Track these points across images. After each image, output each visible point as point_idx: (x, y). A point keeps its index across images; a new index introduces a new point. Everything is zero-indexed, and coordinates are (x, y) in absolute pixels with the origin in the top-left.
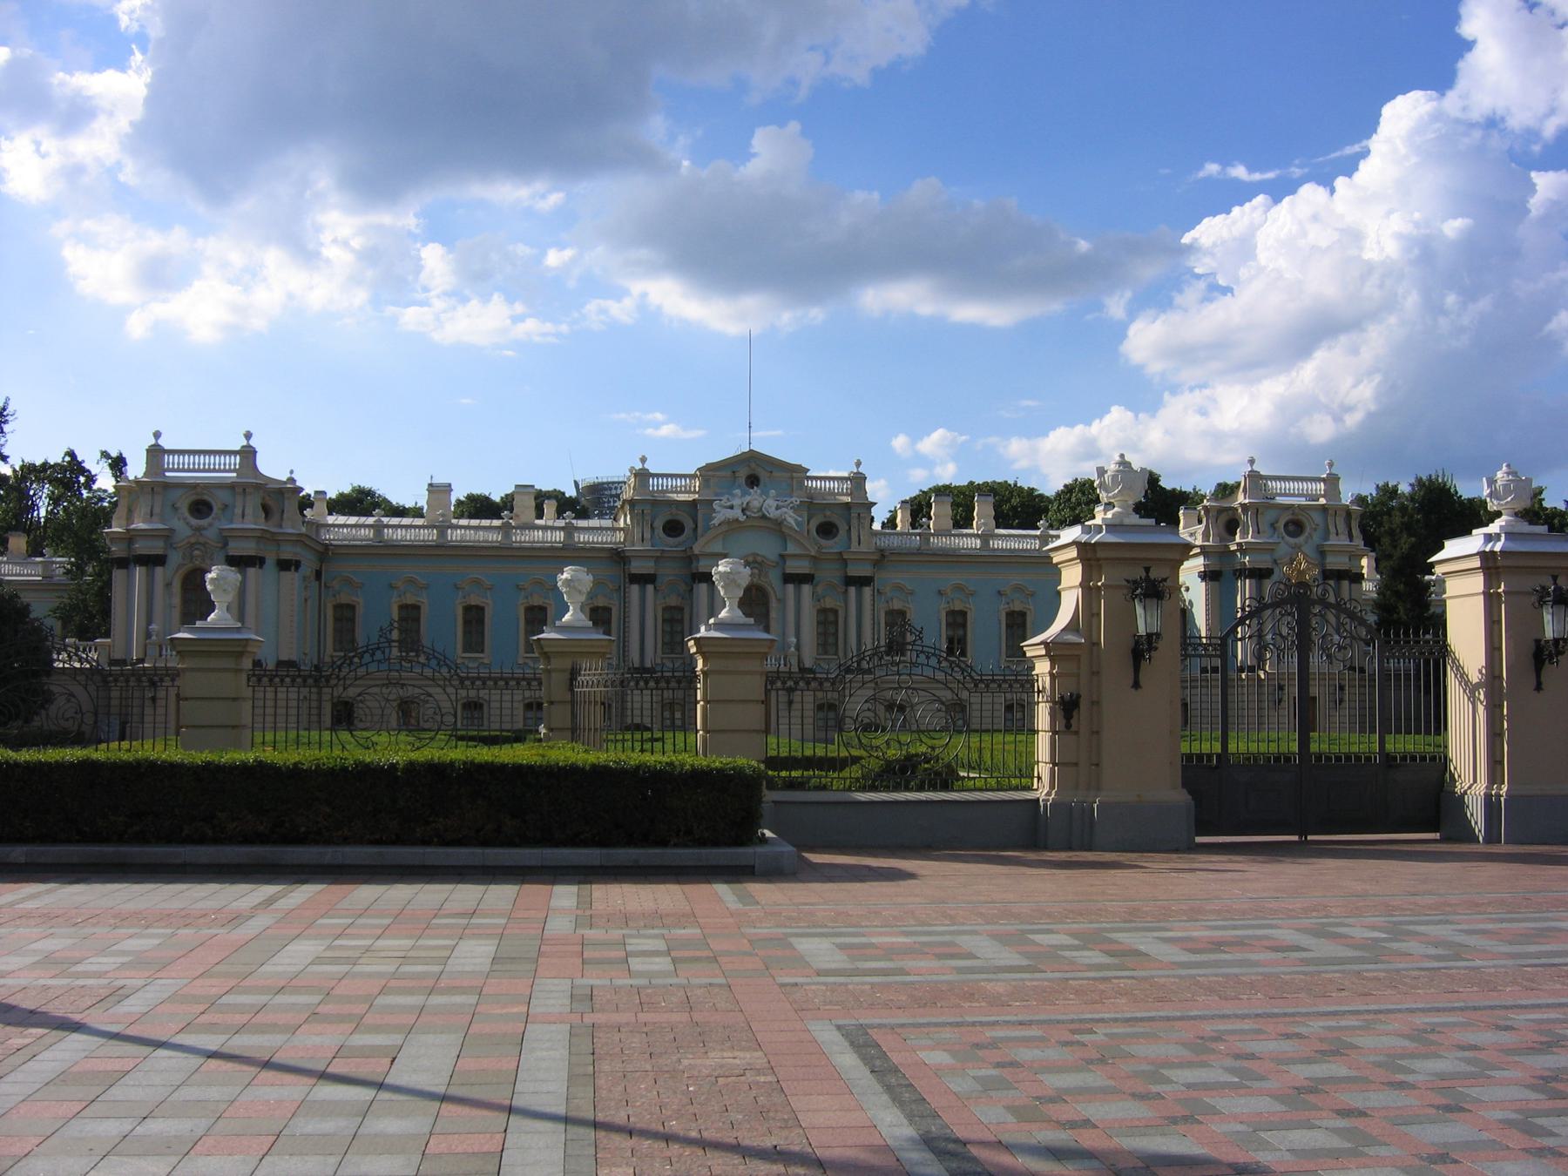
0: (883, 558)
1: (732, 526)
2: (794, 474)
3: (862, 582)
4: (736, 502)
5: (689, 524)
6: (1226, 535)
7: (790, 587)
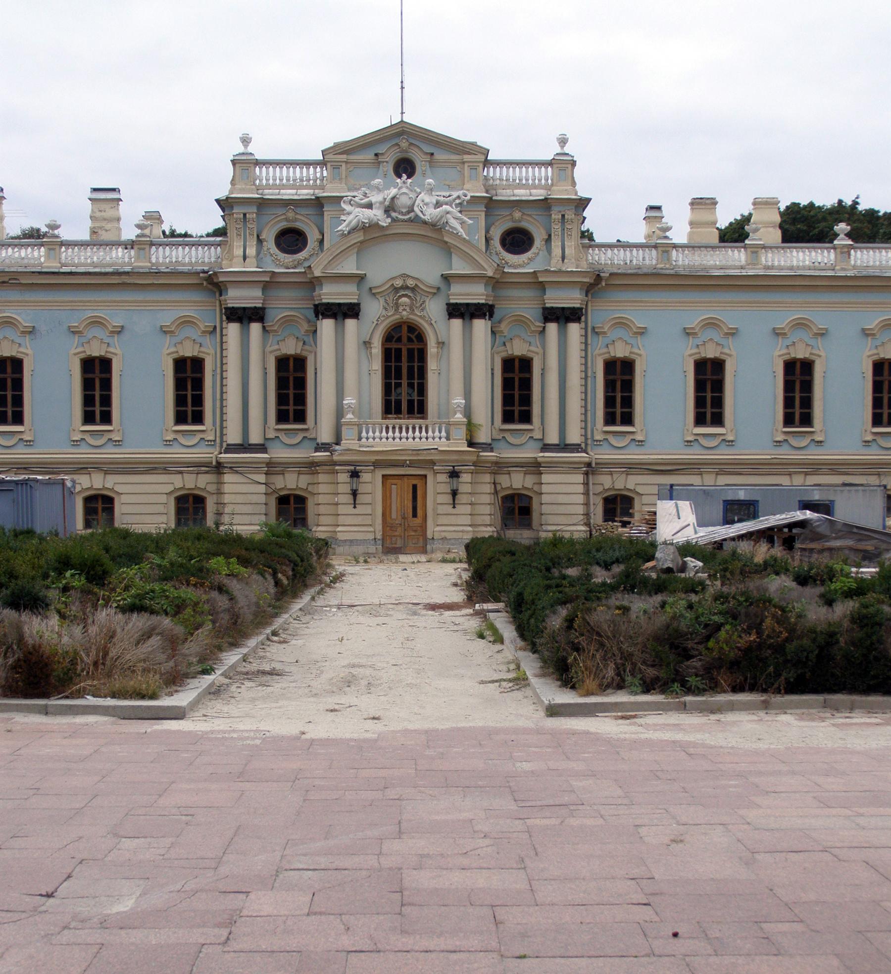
0: (597, 283)
1: (370, 235)
2: (467, 155)
3: (564, 316)
4: (376, 198)
5: (312, 236)
7: (457, 323)
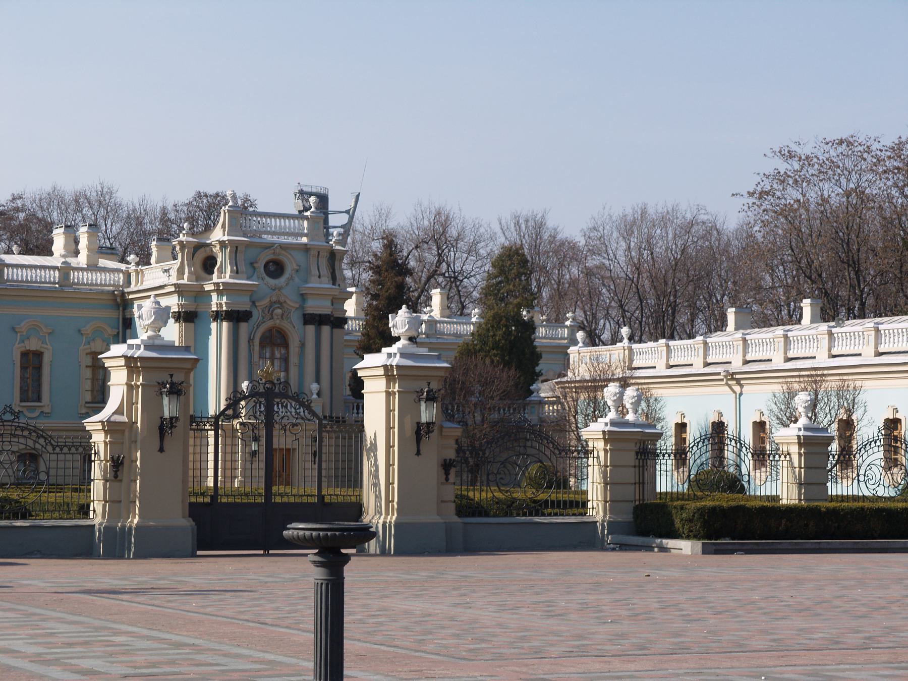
6: (203, 274)
